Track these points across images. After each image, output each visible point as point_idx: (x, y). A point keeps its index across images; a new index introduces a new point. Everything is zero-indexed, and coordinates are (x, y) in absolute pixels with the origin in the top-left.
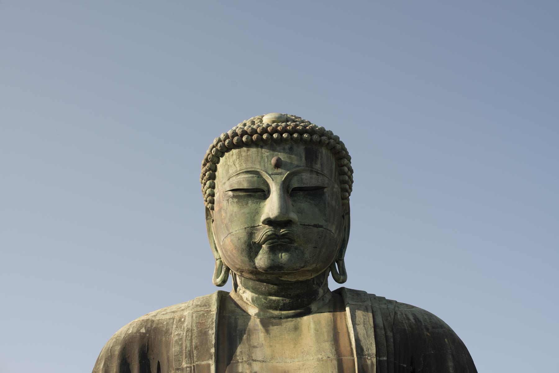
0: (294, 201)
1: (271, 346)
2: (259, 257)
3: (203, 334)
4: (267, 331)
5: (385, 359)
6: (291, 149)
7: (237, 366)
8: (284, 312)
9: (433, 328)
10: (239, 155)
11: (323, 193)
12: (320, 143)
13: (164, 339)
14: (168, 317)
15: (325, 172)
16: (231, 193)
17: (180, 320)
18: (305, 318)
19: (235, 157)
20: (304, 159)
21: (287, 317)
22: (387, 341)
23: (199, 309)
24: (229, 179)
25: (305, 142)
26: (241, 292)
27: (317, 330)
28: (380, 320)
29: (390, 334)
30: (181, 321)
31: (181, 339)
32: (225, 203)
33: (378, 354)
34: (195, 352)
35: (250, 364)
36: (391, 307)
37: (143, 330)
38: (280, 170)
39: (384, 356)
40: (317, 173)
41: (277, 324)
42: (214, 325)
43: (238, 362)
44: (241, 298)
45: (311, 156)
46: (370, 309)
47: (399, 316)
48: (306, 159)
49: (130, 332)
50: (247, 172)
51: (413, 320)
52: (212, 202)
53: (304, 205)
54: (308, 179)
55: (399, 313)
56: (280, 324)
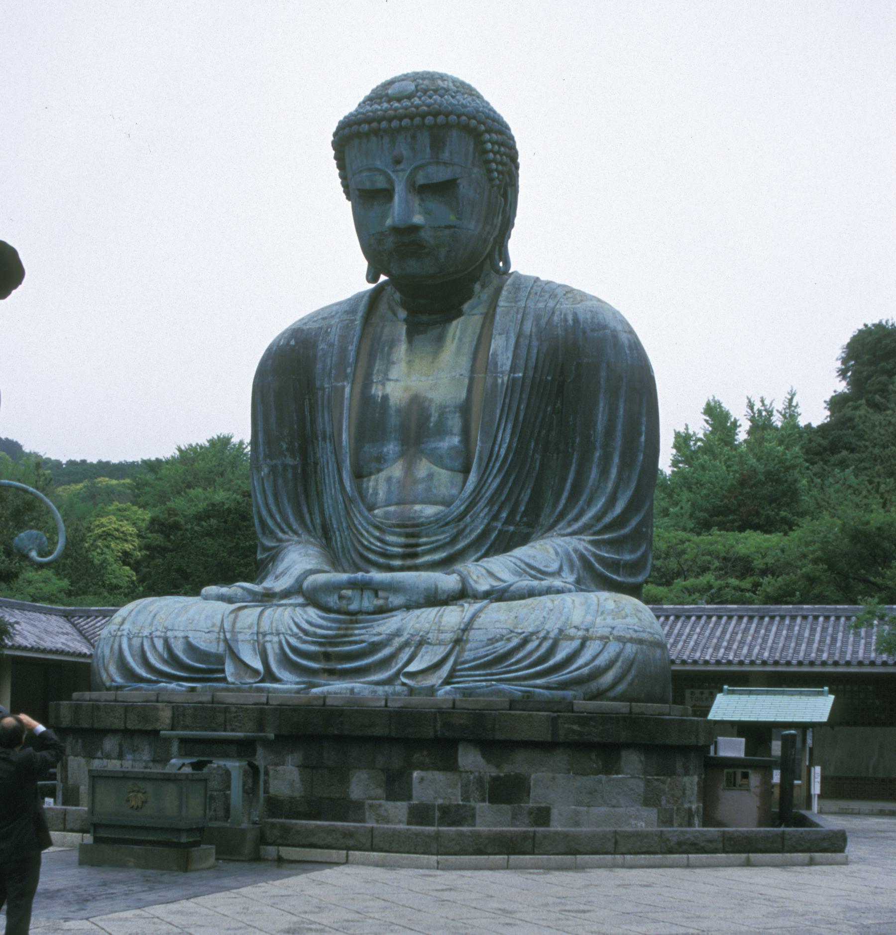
0: (422, 200)
1: (410, 361)
2: (392, 265)
3: (343, 350)
5: (521, 375)
6: (414, 137)
7: (371, 387)
9: (593, 330)
11: (457, 186)
12: (447, 126)
16: (357, 192)
17: (326, 331)
18: (454, 323)
20: (428, 150)
22: (528, 353)
23: (345, 317)
25: (430, 128)
27: (460, 340)
28: (528, 327)
29: (535, 343)
34: (333, 372)
38: (402, 166)
39: (519, 372)
40: (445, 164)
43: (372, 382)
45: (437, 144)
46: (521, 311)
47: (556, 319)
48: (431, 148)
50: (369, 170)
51: (570, 322)
53: (435, 205)
55: (557, 313)
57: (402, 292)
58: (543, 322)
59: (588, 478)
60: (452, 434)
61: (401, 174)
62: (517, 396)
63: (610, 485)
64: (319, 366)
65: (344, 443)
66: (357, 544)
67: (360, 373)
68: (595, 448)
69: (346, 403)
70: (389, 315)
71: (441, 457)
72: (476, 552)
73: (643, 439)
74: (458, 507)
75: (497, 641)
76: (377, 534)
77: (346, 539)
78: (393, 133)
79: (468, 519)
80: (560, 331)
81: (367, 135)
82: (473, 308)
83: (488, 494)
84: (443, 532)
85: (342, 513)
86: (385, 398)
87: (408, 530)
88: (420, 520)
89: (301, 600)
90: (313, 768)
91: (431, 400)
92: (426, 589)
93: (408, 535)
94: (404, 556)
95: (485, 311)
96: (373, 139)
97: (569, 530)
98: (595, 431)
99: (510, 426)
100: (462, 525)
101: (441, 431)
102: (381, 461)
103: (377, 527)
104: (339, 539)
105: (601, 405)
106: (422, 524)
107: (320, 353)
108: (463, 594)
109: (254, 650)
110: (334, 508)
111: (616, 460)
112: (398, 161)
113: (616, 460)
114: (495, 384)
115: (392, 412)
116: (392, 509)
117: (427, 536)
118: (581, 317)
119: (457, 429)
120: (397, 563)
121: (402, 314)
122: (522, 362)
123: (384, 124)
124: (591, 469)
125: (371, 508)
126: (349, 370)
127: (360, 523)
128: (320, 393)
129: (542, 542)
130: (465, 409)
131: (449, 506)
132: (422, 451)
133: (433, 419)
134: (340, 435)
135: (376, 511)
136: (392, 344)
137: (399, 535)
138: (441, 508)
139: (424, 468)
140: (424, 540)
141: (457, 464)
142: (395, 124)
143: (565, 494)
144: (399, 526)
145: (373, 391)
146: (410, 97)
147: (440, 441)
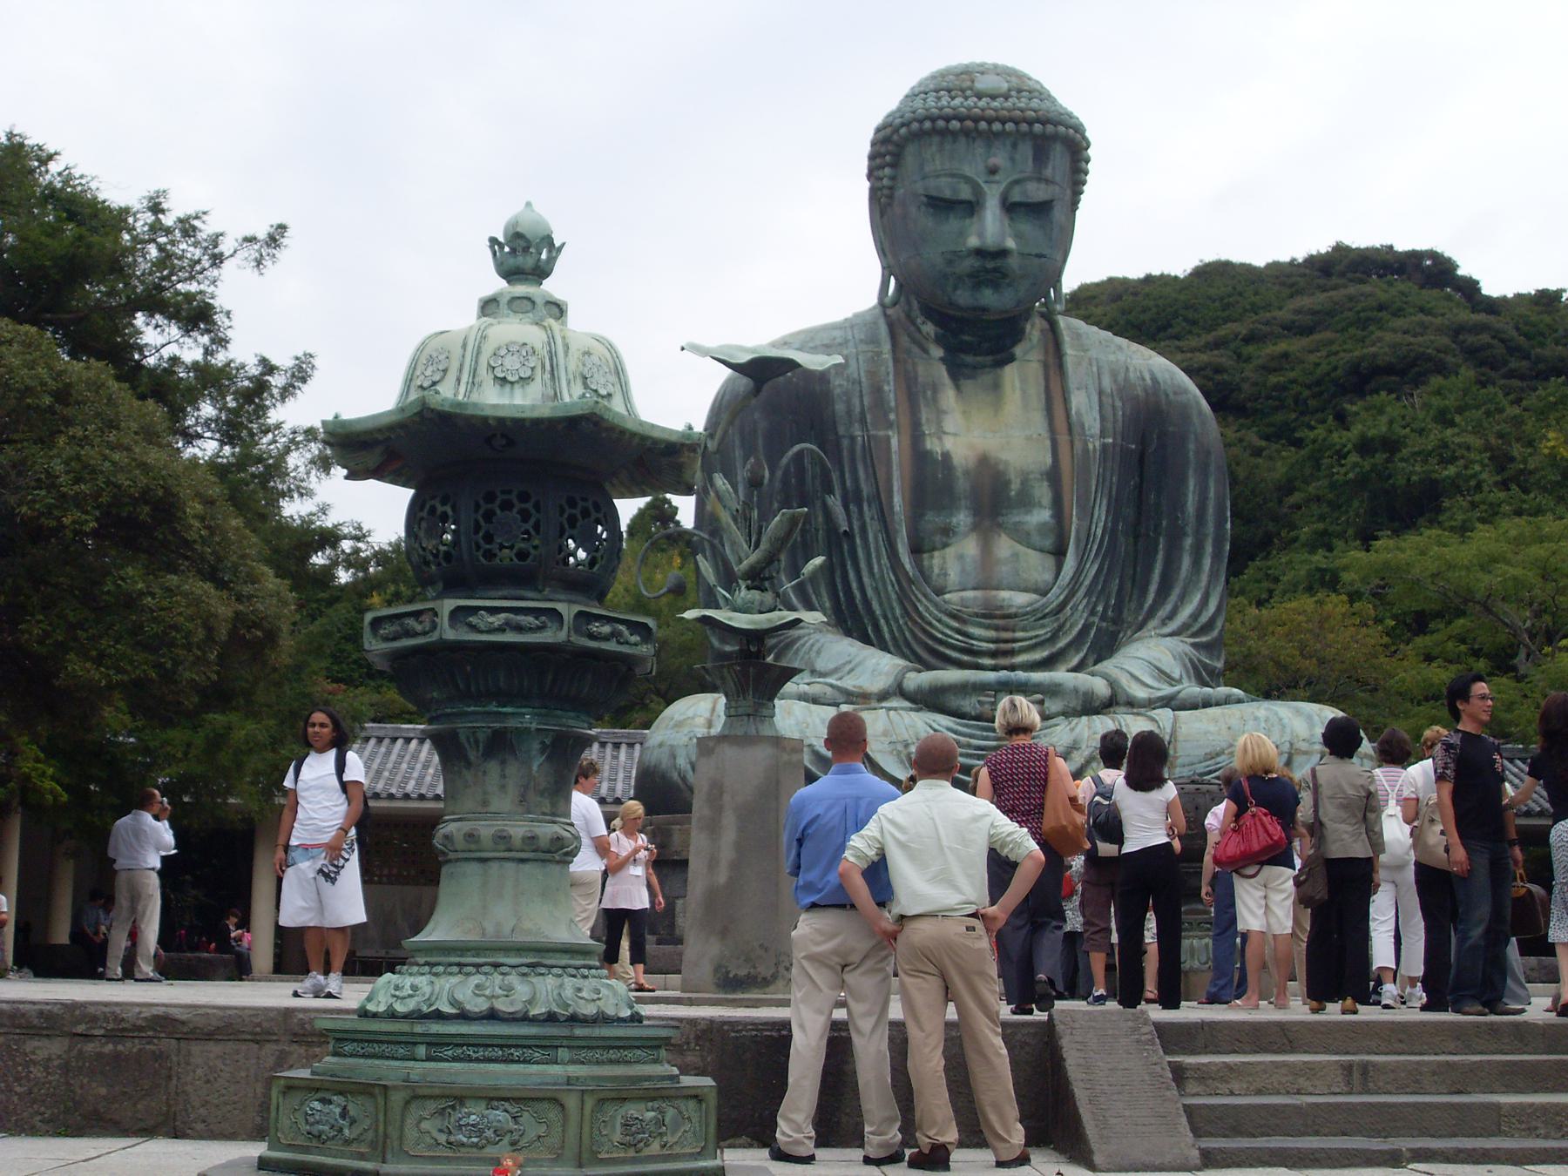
0: (1011, 219)
1: (964, 412)
3: (877, 390)
4: (958, 387)
6: (1014, 146)
8: (979, 359)
9: (1175, 393)
12: (1055, 137)
13: (817, 388)
15: (1058, 179)
19: (934, 148)
21: (984, 367)
24: (924, 178)
26: (919, 321)
27: (1024, 392)
28: (1107, 383)
29: (1118, 404)
31: (847, 393)
32: (913, 210)
33: (1103, 434)
34: (869, 418)
35: (940, 439)
36: (1121, 357)
38: (997, 177)
40: (1047, 181)
41: (969, 377)
42: (891, 377)
44: (919, 330)
45: (1041, 156)
47: (1132, 375)
50: (953, 175)
51: (1149, 382)
52: (891, 197)
53: (1027, 227)
54: (1036, 192)
56: (972, 377)
57: (936, 324)
58: (1121, 378)
59: (1179, 568)
60: (1040, 506)
61: (994, 186)
62: (1109, 464)
63: (1204, 578)
64: (840, 407)
65: (897, 508)
66: (920, 635)
67: (905, 421)
68: (1185, 534)
69: (895, 457)
70: (916, 350)
71: (1028, 534)
72: (1078, 651)
73: (1229, 526)
74: (1055, 596)
75: (1218, 755)
76: (956, 624)
77: (899, 627)
78: (991, 138)
79: (1068, 609)
80: (1140, 391)
81: (954, 134)
82: (1026, 353)
83: (1087, 583)
84: (1043, 626)
85: (894, 596)
86: (946, 456)
87: (996, 621)
88: (1013, 610)
89: (907, 704)
91: (1007, 463)
92: (1085, 694)
93: (997, 629)
94: (993, 654)
95: (1041, 357)
96: (963, 139)
97: (1167, 630)
98: (1183, 513)
99: (1105, 502)
100: (1062, 617)
101: (1026, 501)
102: (948, 532)
104: (885, 629)
105: (1191, 484)
106: (1015, 616)
107: (837, 391)
108: (1114, 701)
109: (902, 762)
110: (876, 590)
111: (1209, 549)
112: (993, 171)
113: (1209, 549)
114: (1086, 450)
115: (959, 473)
116: (970, 594)
117: (1024, 629)
118: (1159, 376)
120: (987, 661)
121: (937, 352)
122: (1109, 425)
123: (983, 125)
124: (1180, 559)
125: (940, 591)
126: (892, 417)
127: (927, 609)
128: (845, 443)
129: (1152, 642)
130: (1053, 476)
131: (1044, 594)
132: (1000, 526)
133: (1015, 487)
134: (890, 497)
135: (947, 596)
136: (935, 389)
137: (988, 627)
138: (1034, 596)
139: (1004, 546)
140: (1020, 634)
141: (1048, 543)
142: (997, 126)
143: (1153, 588)
145: (928, 446)
146: (1006, 97)
147: (1029, 512)
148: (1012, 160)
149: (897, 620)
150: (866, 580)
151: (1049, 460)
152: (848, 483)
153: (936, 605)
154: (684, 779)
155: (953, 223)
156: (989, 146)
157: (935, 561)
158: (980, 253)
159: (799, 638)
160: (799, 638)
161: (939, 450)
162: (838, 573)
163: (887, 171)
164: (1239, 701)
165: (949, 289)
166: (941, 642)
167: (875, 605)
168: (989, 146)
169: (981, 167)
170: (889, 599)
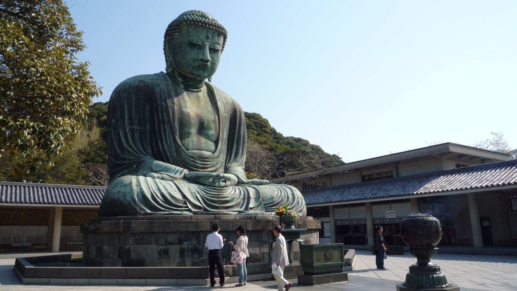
4: (189, 96)
6: (213, 33)
10: (195, 28)
14: (151, 81)
19: (193, 29)
28: (224, 100)
30: (158, 85)
37: (142, 85)
38: (209, 40)
44: (177, 80)
49: (136, 84)
64: (158, 96)
86: (188, 113)
90: (260, 242)
94: (202, 168)
96: (201, 28)
103: (192, 157)
110: (168, 148)
112: (208, 38)
115: (192, 118)
119: (214, 128)
125: (187, 150)
128: (160, 106)
133: (206, 124)
137: (201, 161)
139: (203, 140)
140: (209, 163)
144: (199, 157)
148: (213, 36)
149: (174, 157)
150: (165, 145)
151: (214, 118)
152: (160, 118)
153: (186, 153)
154: (130, 204)
155: (195, 51)
156: (207, 32)
157: (186, 141)
158: (202, 60)
159: (145, 160)
160: (145, 160)
161: (186, 111)
162: (154, 143)
163: (177, 34)
164: (268, 184)
165: (191, 69)
166: (188, 164)
167: (168, 152)
168: (207, 32)
169: (205, 37)
170: (172, 151)
